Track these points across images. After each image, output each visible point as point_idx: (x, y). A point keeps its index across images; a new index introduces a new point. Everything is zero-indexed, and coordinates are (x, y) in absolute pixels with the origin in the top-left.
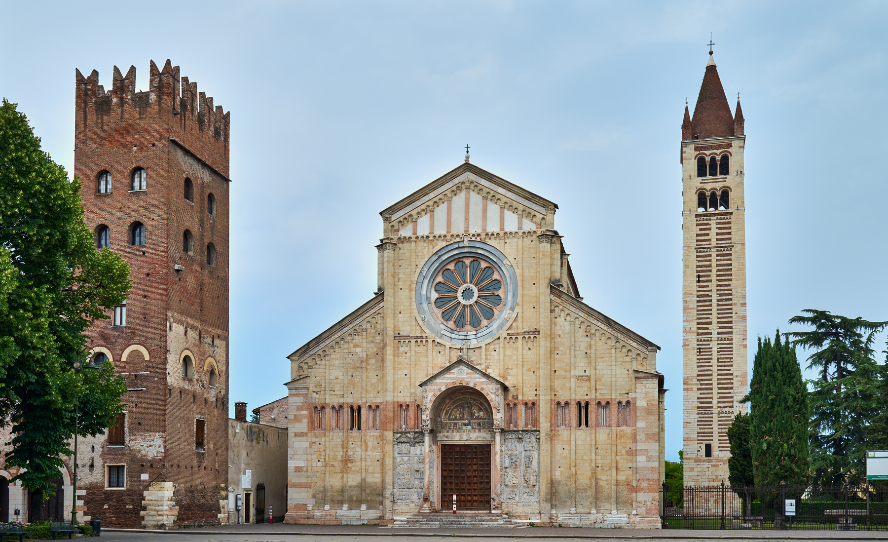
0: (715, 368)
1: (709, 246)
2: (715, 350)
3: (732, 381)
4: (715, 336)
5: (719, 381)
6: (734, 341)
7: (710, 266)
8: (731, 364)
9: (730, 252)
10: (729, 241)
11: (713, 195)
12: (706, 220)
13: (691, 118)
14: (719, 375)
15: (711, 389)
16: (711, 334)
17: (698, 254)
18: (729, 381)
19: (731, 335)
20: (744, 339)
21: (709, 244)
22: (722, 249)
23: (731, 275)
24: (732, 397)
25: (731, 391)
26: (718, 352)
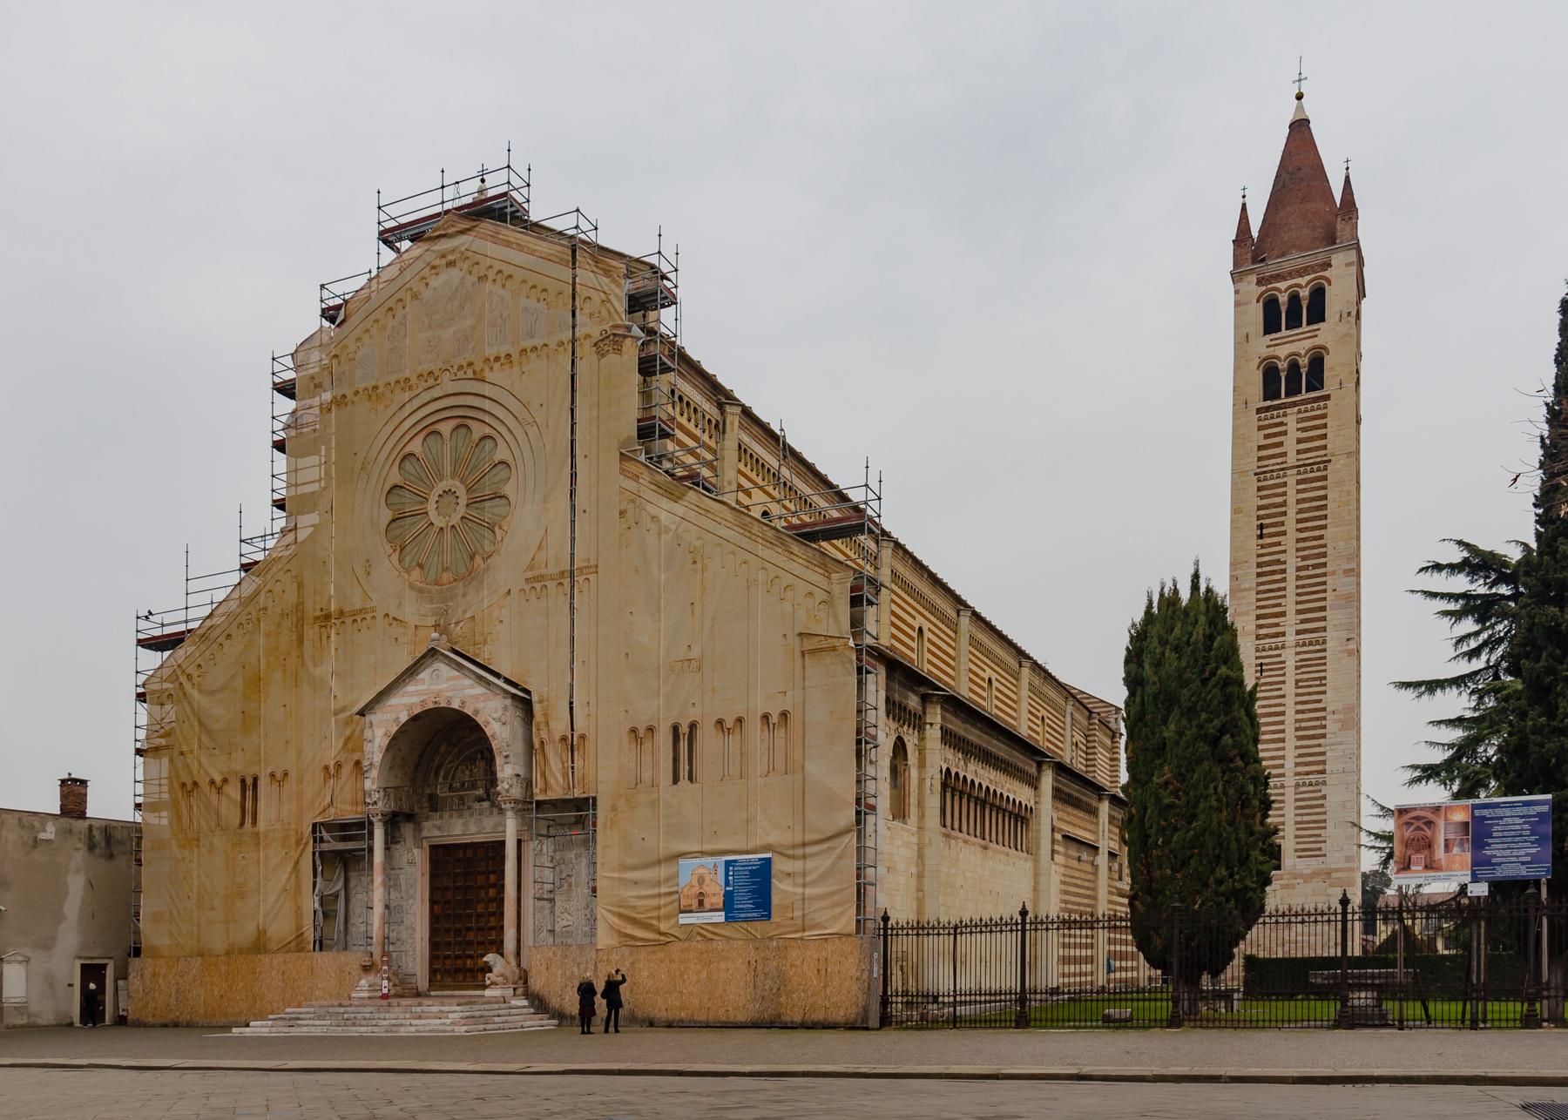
0: (1290, 701)
1: (1282, 466)
2: (1291, 663)
3: (1324, 723)
4: (1291, 638)
5: (1298, 725)
6: (1329, 645)
7: (1284, 504)
8: (1322, 689)
9: (1324, 473)
10: (1323, 452)
11: (1294, 367)
12: (1278, 417)
13: (1255, 234)
14: (1298, 712)
15: (1283, 740)
16: (1283, 634)
17: (1261, 484)
18: (1318, 723)
19: (1323, 634)
20: (1348, 640)
21: (1282, 463)
22: (1308, 468)
23: (1325, 517)
24: (1323, 754)
25: (1321, 741)
26: (1297, 668)
